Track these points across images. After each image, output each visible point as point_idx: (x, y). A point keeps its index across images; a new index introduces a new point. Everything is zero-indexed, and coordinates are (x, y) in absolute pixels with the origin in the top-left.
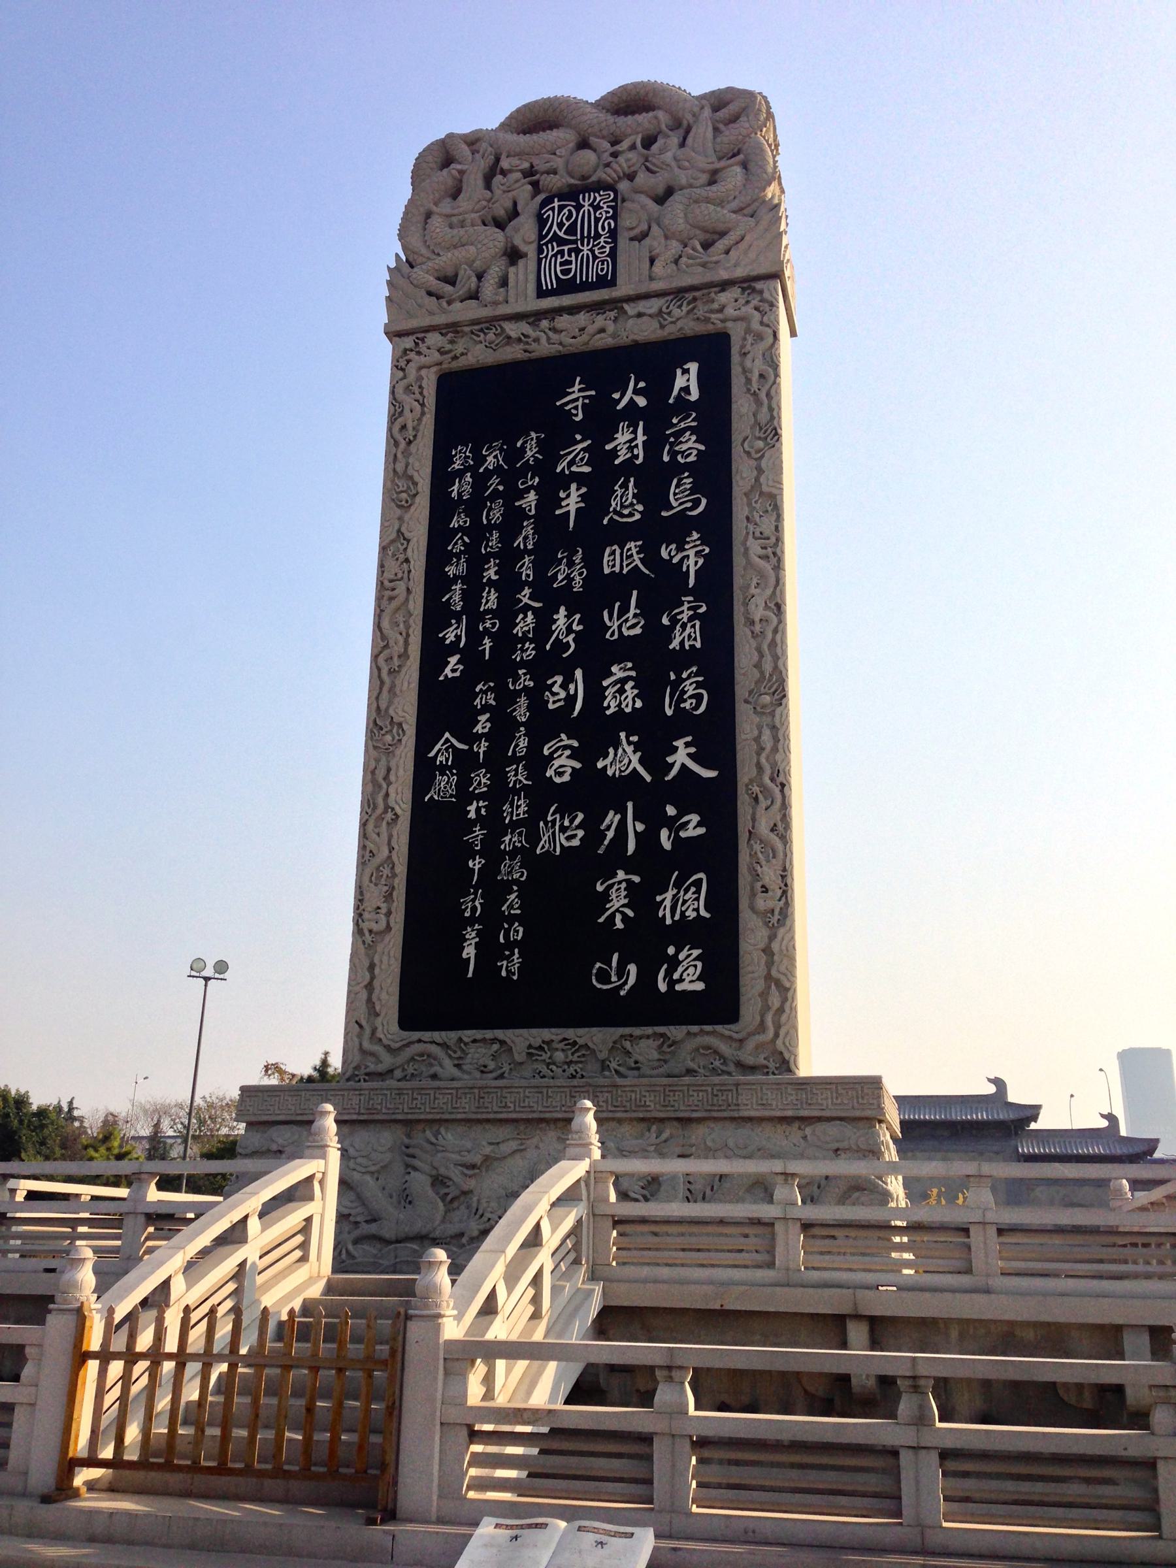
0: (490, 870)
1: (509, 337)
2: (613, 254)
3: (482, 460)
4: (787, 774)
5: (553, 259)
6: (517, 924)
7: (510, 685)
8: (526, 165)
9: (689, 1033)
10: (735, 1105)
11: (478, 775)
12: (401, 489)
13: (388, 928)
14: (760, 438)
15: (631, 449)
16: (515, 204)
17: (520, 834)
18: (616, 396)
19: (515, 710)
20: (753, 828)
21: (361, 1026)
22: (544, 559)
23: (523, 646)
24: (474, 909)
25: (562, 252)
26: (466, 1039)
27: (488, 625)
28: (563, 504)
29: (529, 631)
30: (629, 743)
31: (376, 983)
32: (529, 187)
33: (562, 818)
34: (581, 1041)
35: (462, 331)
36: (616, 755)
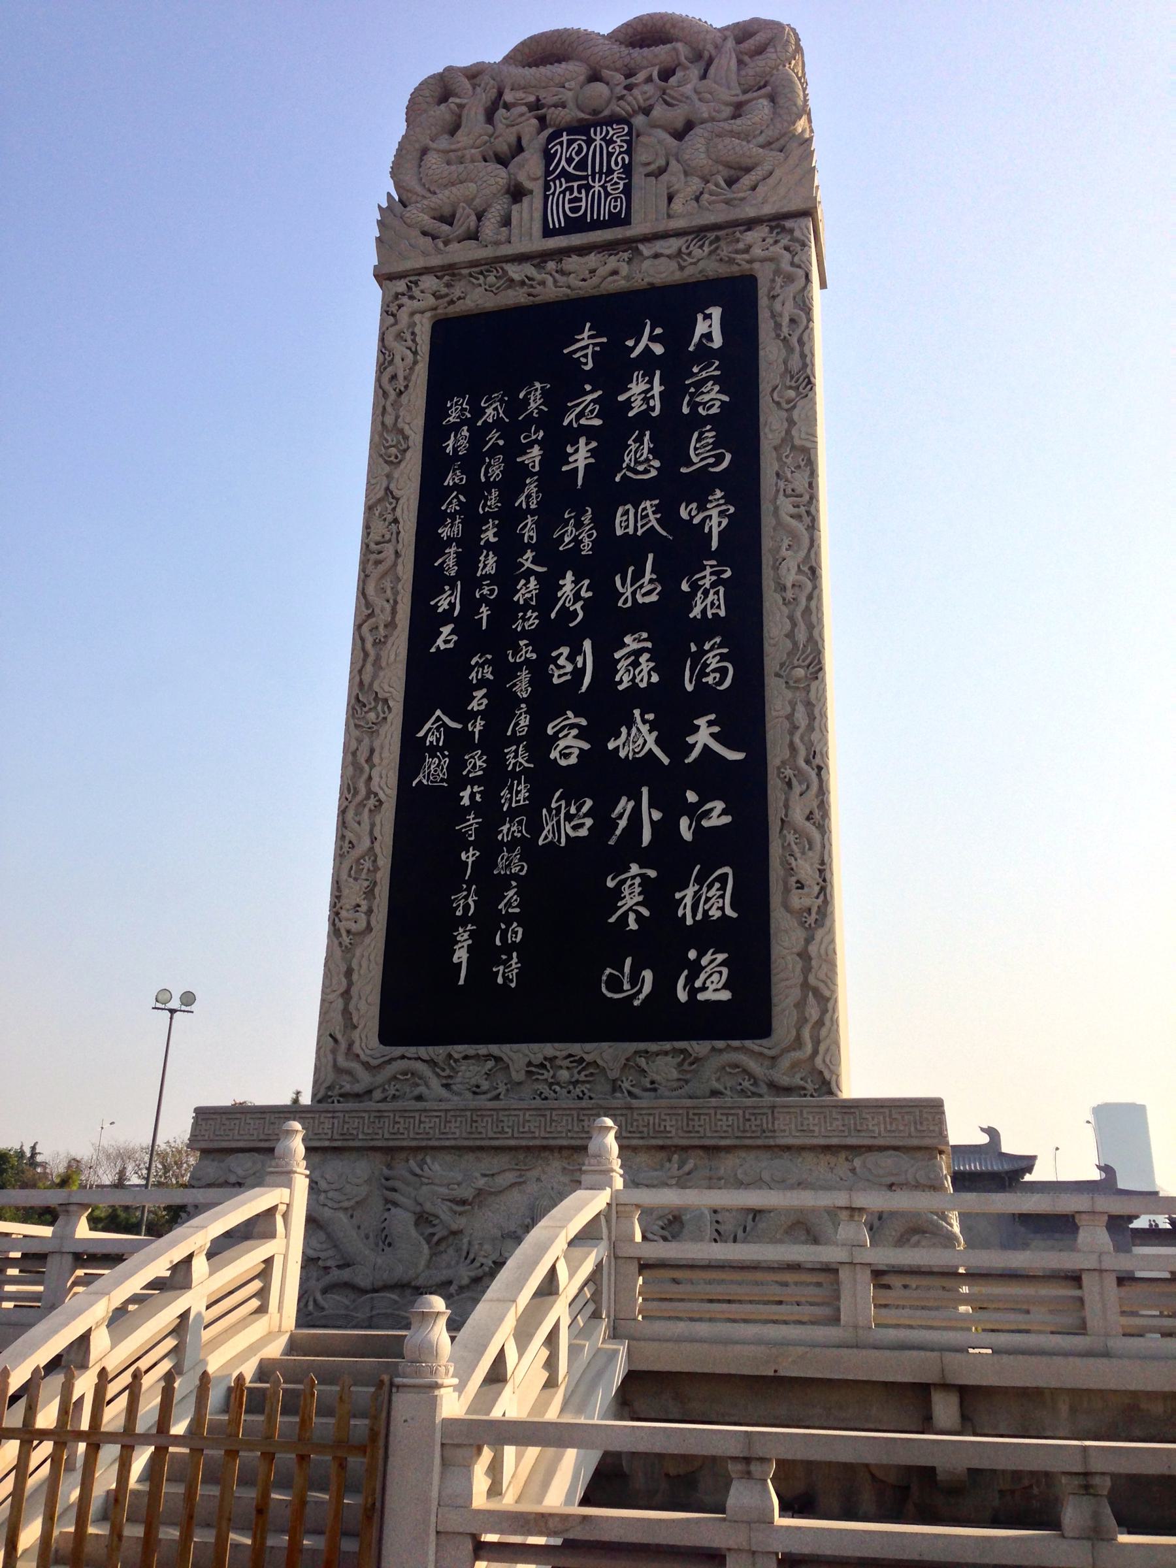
0: (485, 864)
1: (512, 280)
2: (627, 191)
3: (479, 412)
4: (825, 755)
5: (561, 196)
6: (515, 924)
7: (510, 658)
8: (532, 99)
9: (713, 1049)
10: (771, 1131)
11: (473, 757)
12: (390, 443)
13: (369, 928)
14: (791, 388)
15: (646, 400)
16: (519, 139)
17: (520, 823)
18: (630, 343)
19: (515, 685)
20: (786, 815)
21: (336, 1040)
22: (549, 519)
23: (525, 614)
24: (467, 907)
25: (571, 189)
26: (456, 1056)
27: (485, 592)
28: (571, 459)
29: (531, 598)
30: (644, 722)
31: (354, 991)
32: (535, 122)
33: (568, 805)
34: (588, 1058)
35: (460, 274)
36: (629, 734)
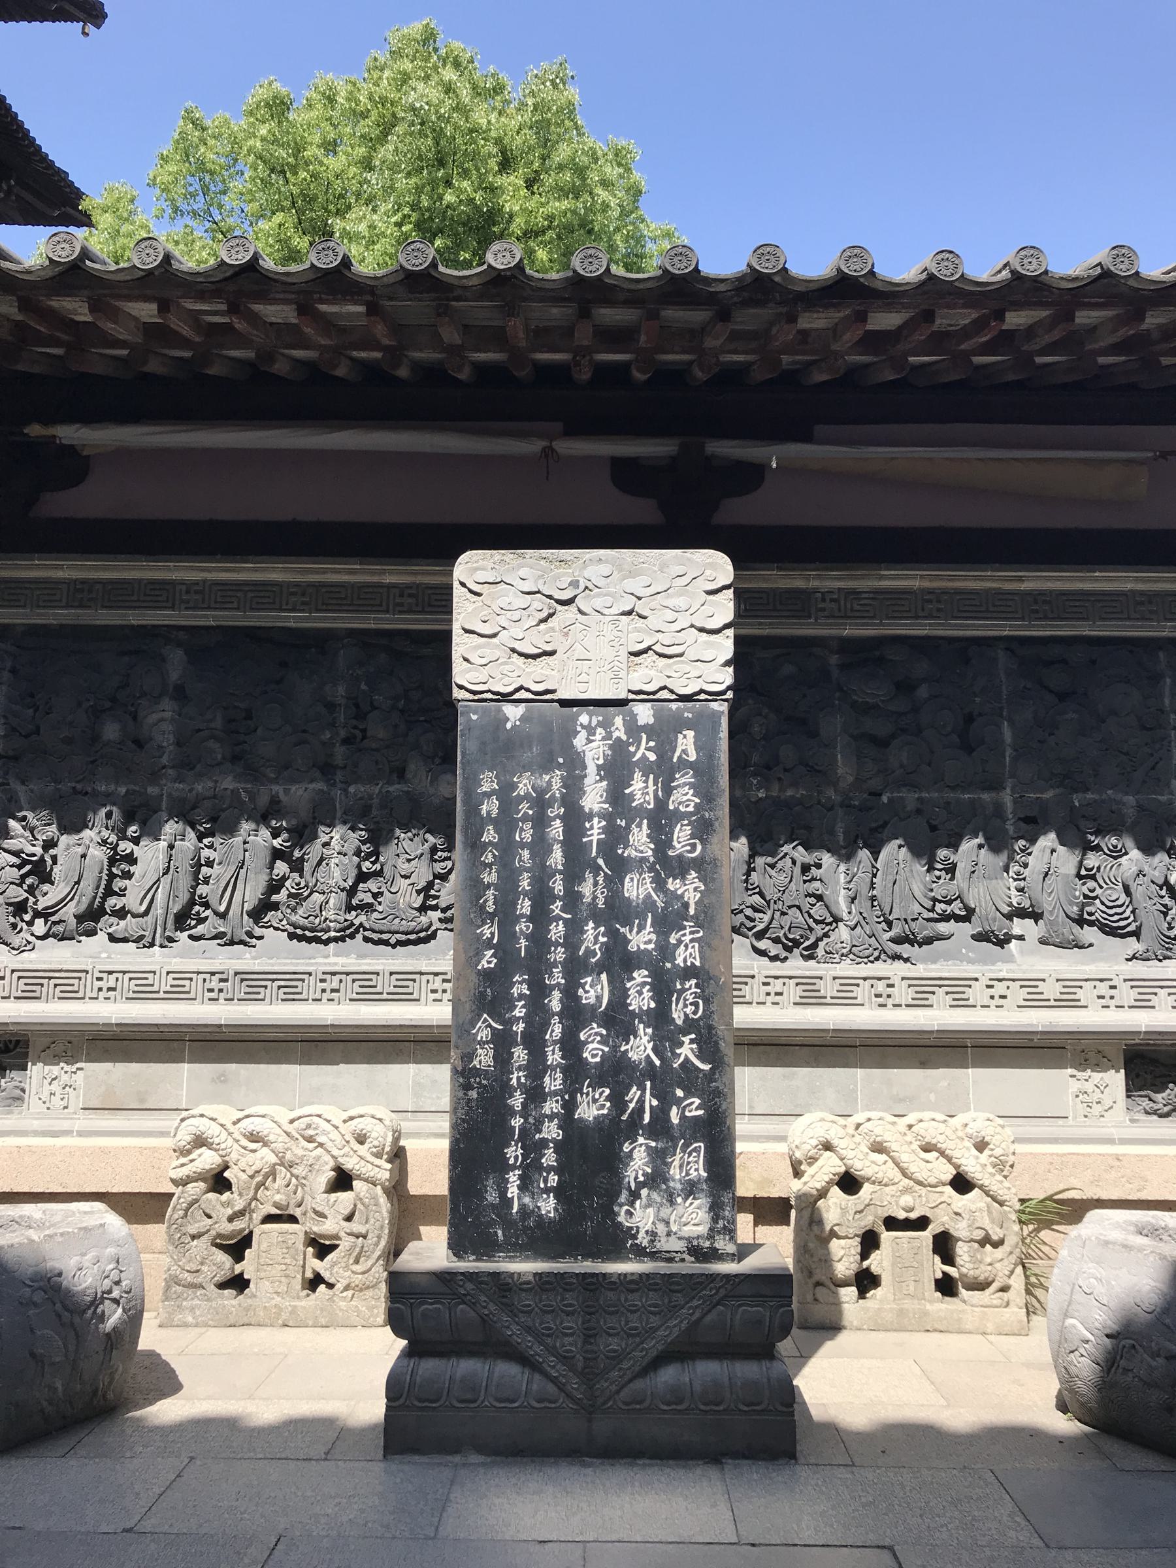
19: (550, 1001)
29: (560, 938)
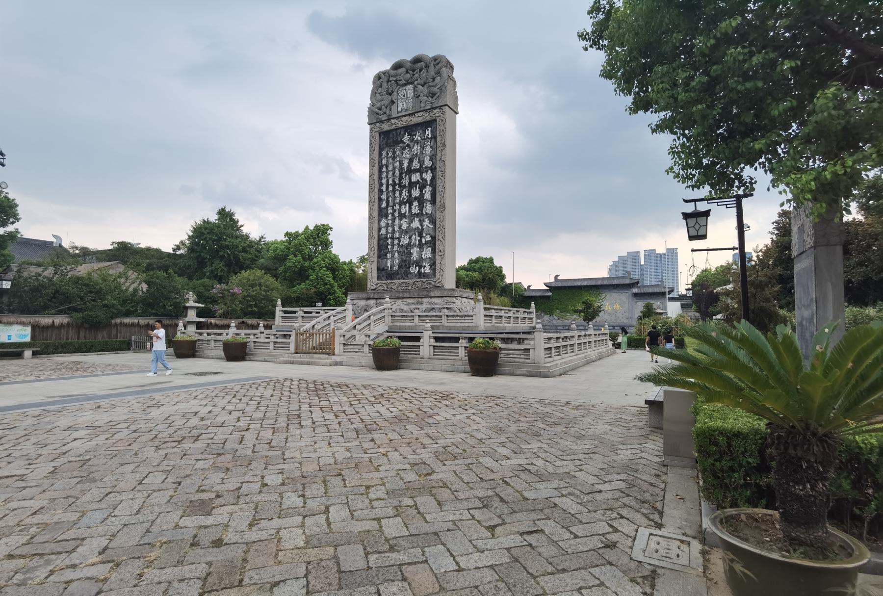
3: (388, 154)
22: (401, 178)
